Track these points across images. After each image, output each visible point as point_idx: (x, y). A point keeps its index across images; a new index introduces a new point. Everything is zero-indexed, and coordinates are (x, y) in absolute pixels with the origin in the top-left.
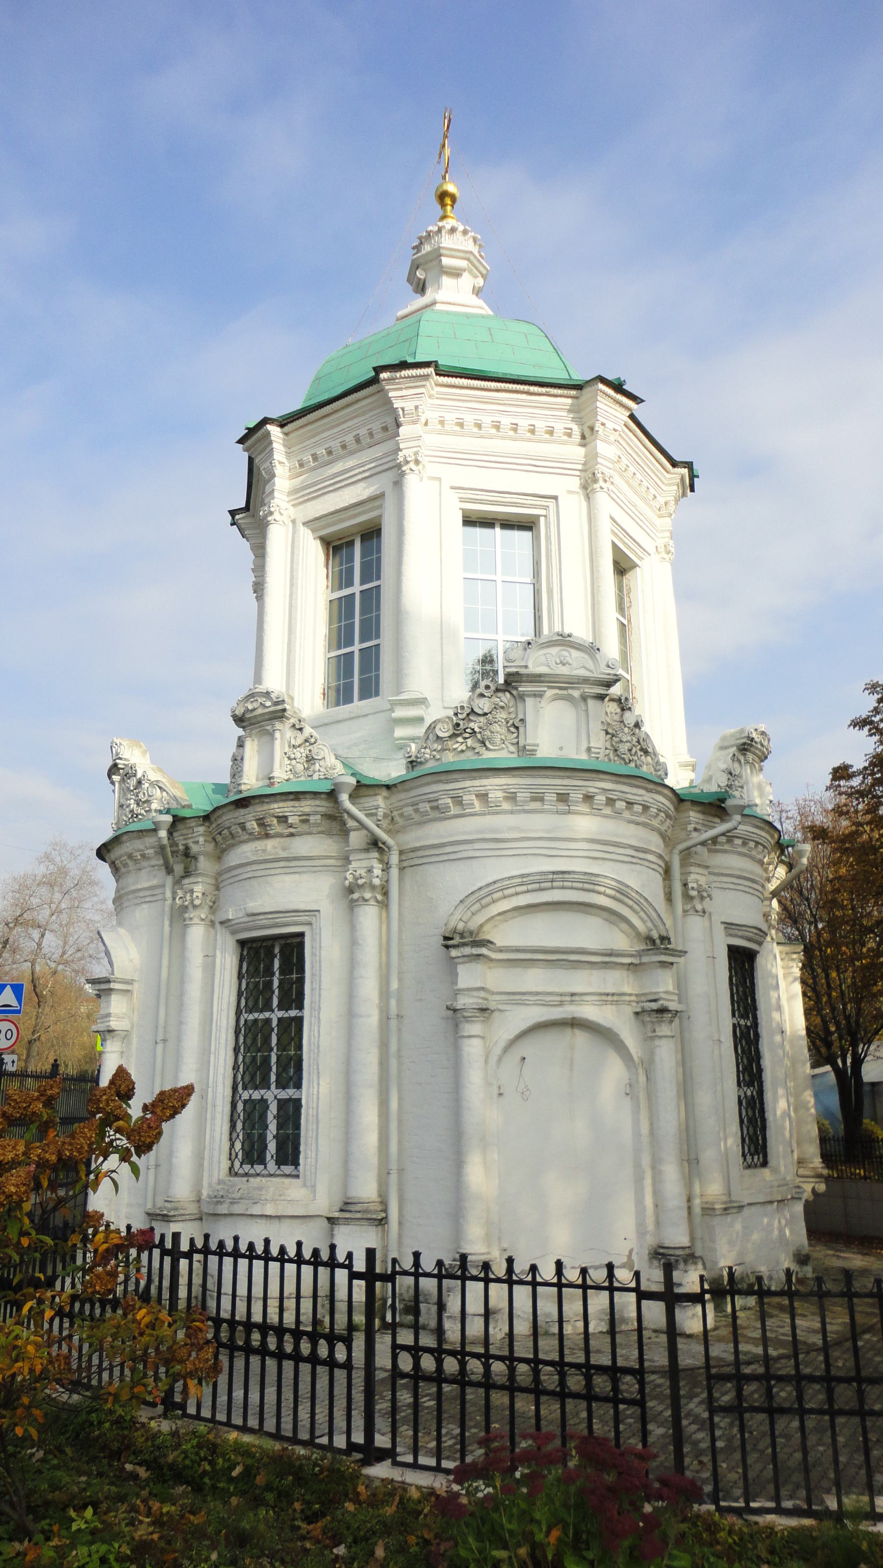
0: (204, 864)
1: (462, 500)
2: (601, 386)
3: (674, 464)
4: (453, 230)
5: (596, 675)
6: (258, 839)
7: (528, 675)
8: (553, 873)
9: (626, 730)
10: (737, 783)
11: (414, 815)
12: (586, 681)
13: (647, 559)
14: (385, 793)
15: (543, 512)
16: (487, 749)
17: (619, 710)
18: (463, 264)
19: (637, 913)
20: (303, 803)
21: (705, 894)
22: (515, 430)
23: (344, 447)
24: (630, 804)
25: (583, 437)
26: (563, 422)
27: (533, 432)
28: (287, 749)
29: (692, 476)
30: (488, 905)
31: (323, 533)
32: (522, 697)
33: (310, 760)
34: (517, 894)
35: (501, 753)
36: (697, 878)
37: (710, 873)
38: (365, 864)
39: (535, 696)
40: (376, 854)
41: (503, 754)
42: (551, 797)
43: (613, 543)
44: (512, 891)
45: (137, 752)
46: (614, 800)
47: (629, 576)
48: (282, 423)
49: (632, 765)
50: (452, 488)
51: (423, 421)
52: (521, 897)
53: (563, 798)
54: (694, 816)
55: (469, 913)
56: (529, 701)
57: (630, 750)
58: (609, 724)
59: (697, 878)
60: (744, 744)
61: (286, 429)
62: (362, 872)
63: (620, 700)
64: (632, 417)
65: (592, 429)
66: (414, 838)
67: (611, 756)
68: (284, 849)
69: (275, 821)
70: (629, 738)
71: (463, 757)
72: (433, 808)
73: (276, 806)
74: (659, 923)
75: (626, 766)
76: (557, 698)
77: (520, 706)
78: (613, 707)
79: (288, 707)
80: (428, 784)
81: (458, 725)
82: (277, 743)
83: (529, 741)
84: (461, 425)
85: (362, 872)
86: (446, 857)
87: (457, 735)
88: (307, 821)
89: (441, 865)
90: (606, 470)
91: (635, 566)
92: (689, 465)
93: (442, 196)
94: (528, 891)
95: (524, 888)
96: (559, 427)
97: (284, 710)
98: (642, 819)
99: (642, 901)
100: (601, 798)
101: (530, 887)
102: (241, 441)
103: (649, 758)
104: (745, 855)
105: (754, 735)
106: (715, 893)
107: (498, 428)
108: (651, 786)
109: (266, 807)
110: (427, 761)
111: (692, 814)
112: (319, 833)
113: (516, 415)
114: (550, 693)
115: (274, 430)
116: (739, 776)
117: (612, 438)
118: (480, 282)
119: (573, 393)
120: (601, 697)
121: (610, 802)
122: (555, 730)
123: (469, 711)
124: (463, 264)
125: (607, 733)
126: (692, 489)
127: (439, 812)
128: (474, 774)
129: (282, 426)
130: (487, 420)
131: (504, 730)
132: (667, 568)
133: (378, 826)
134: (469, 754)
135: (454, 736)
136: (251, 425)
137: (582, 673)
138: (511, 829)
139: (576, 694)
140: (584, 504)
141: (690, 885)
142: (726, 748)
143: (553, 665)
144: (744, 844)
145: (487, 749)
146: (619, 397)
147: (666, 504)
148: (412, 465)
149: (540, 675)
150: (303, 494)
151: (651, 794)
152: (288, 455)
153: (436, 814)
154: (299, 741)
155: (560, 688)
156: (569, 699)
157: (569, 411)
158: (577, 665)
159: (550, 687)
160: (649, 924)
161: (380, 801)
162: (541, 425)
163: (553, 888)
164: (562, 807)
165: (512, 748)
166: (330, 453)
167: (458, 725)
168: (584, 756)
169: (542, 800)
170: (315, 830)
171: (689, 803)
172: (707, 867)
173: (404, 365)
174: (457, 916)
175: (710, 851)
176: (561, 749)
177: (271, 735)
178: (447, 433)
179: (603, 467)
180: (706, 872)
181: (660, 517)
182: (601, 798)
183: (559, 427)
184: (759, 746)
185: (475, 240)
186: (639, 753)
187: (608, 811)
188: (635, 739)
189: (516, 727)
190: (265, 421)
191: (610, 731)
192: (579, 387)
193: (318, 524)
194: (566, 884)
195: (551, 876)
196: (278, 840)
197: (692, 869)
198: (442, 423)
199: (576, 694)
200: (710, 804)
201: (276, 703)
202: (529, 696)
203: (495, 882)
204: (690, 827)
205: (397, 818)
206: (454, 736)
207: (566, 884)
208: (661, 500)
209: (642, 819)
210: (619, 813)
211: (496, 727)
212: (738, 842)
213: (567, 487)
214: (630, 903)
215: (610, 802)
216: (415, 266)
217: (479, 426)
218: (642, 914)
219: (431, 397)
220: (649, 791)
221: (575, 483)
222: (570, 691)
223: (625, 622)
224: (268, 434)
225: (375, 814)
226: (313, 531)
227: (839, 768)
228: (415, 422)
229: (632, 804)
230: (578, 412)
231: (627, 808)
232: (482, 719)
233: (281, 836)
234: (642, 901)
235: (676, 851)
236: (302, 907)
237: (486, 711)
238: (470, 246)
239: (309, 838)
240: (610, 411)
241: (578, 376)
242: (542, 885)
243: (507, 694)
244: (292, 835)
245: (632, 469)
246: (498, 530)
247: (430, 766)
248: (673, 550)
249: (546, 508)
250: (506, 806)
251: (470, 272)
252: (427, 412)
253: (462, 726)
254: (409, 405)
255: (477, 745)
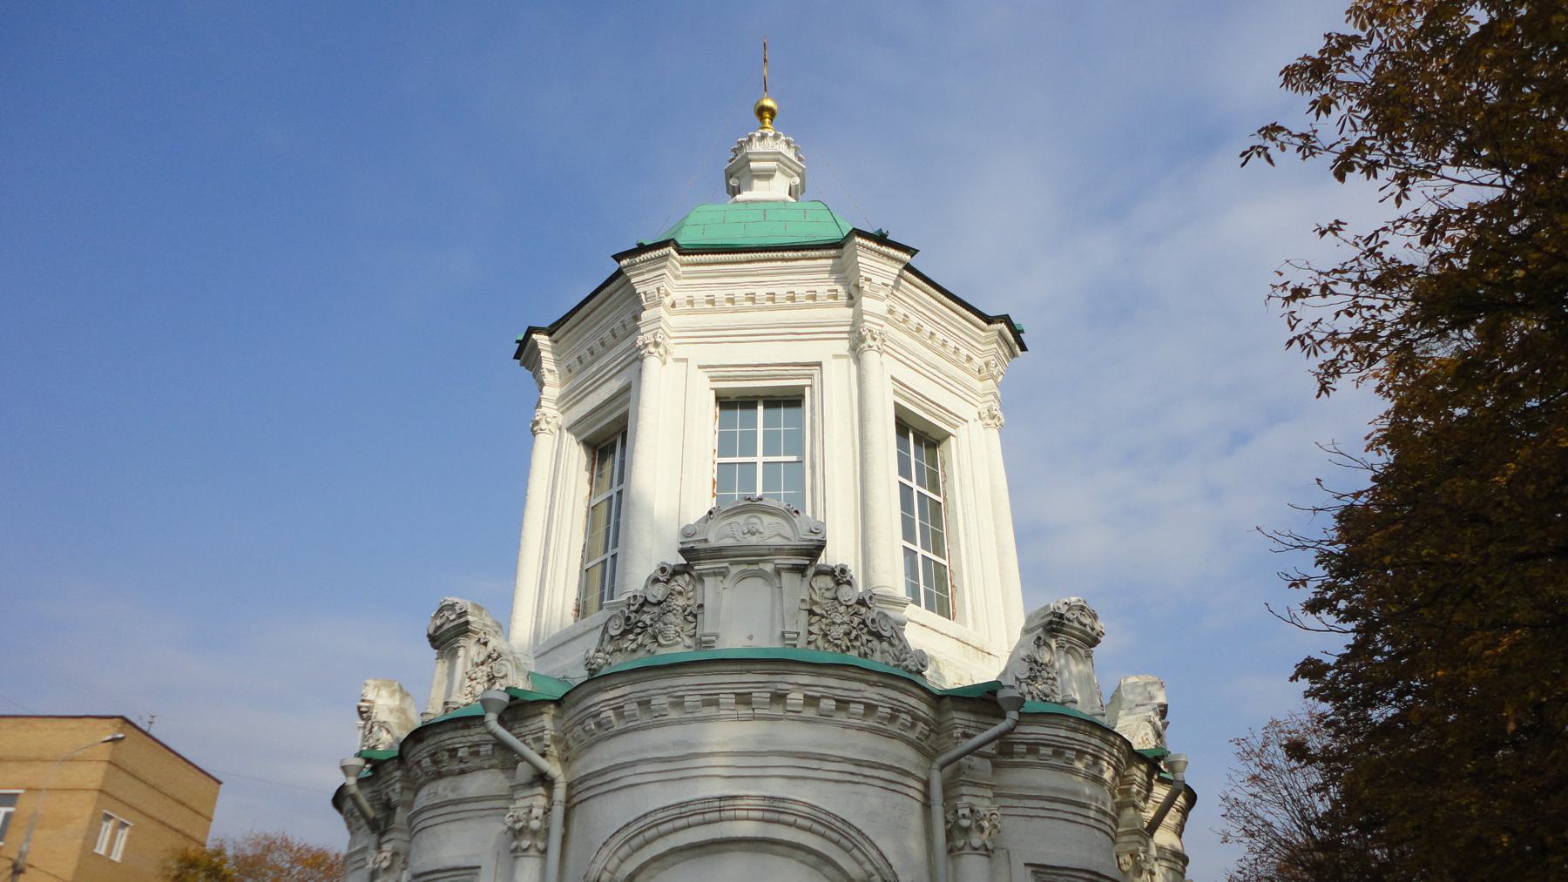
0: (401, 816)
1: (713, 379)
2: (858, 240)
3: (990, 320)
4: (763, 137)
5: (795, 543)
6: (433, 779)
7: (705, 550)
8: (720, 799)
9: (842, 609)
10: (1044, 674)
11: (583, 736)
12: (778, 550)
13: (963, 428)
14: (552, 709)
15: (807, 382)
16: (660, 645)
17: (831, 584)
18: (773, 165)
19: (848, 851)
20: (472, 731)
21: (986, 824)
22: (773, 300)
23: (603, 344)
24: (842, 704)
25: (850, 297)
26: (825, 285)
27: (793, 299)
28: (469, 667)
29: (1017, 333)
30: (640, 847)
31: (585, 436)
32: (700, 578)
33: (492, 679)
34: (676, 830)
35: (679, 647)
36: (975, 800)
37: (996, 795)
38: (526, 802)
39: (715, 574)
40: (541, 790)
41: (679, 649)
42: (727, 699)
43: (896, 404)
44: (669, 826)
45: (384, 692)
46: (817, 699)
47: (943, 447)
48: (550, 332)
49: (854, 653)
50: (700, 367)
51: (667, 301)
52: (680, 834)
53: (744, 699)
54: (960, 719)
55: (615, 861)
56: (709, 581)
57: (847, 634)
58: (816, 603)
59: (975, 800)
60: (1051, 622)
61: (555, 336)
62: (521, 813)
63: (833, 571)
64: (908, 268)
65: (857, 286)
66: (584, 766)
67: (820, 643)
68: (454, 790)
69: (446, 755)
70: (846, 619)
71: (635, 656)
72: (599, 725)
73: (446, 736)
74: (881, 864)
75: (851, 656)
76: (744, 576)
77: (699, 587)
78: (827, 582)
79: (470, 618)
80: (589, 694)
81: (628, 618)
82: (460, 661)
83: (707, 631)
84: (712, 302)
85: (521, 813)
86: (606, 788)
87: (630, 631)
88: (476, 754)
89: (602, 798)
90: (876, 328)
91: (950, 435)
92: (1006, 319)
93: (761, 111)
94: (689, 826)
95: (683, 822)
96: (822, 290)
97: (467, 623)
98: (870, 722)
99: (852, 833)
100: (796, 697)
101: (693, 820)
102: (517, 356)
103: (885, 644)
104: (1062, 769)
105: (1063, 610)
106: (1008, 824)
107: (753, 300)
108: (874, 678)
109: (437, 739)
110: (601, 667)
111: (954, 714)
112: (491, 767)
113: (774, 283)
114: (734, 570)
115: (542, 340)
116: (1050, 665)
117: (882, 294)
118: (797, 180)
119: (833, 252)
120: (800, 570)
121: (811, 701)
122: (743, 617)
123: (641, 600)
124: (773, 165)
125: (811, 613)
126: (1023, 348)
127: (605, 732)
128: (634, 676)
129: (550, 334)
130: (739, 293)
131: (679, 620)
132: (994, 435)
133: (543, 755)
134: (641, 653)
135: (624, 634)
136: (521, 337)
137: (778, 541)
138: (676, 744)
139: (769, 568)
140: (854, 367)
141: (960, 812)
142: (1032, 630)
143: (739, 536)
144: (1058, 752)
145: (660, 645)
146: (884, 249)
147: (987, 364)
148: (652, 349)
149: (720, 549)
150: (568, 400)
151: (876, 689)
152: (558, 362)
153: (602, 733)
154: (482, 658)
155: (749, 563)
156: (761, 574)
157: (831, 272)
158: (771, 532)
159: (732, 564)
160: (869, 867)
161: (547, 722)
162: (800, 291)
163: (721, 820)
164: (744, 711)
165: (689, 642)
166: (592, 353)
167: (628, 618)
168: (778, 645)
169: (716, 703)
170: (487, 763)
171: (948, 700)
172: (992, 787)
173: (642, 249)
174: (599, 865)
175: (995, 765)
176: (750, 638)
177: (453, 654)
178: (697, 312)
179: (870, 324)
180: (989, 793)
181: (981, 380)
182: (796, 697)
183: (822, 290)
184: (1076, 625)
185: (788, 143)
186: (865, 637)
187: (810, 713)
188: (856, 620)
189: (693, 615)
190: (531, 330)
191: (816, 609)
192: (837, 245)
193: (580, 427)
194: (739, 813)
195: (717, 804)
196: (450, 779)
197: (964, 790)
198: (691, 302)
199: (769, 568)
200: (982, 699)
201: (460, 615)
202: (708, 575)
203: (645, 816)
204: (957, 733)
205: (571, 742)
206: (624, 634)
207: (739, 813)
208: (978, 361)
209: (870, 722)
210: (826, 715)
211: (670, 617)
212: (1043, 750)
213: (831, 352)
214: (836, 836)
215: (811, 701)
216: (729, 175)
217: (732, 301)
218: (855, 852)
219: (677, 277)
220: (874, 684)
221: (843, 346)
222: (762, 566)
223: (940, 500)
224: (535, 343)
225: (540, 739)
226: (577, 435)
227: (1303, 664)
228: (658, 304)
229: (848, 702)
230: (842, 271)
231: (838, 708)
232: (656, 610)
233: (451, 774)
234: (852, 833)
235: (936, 766)
236: (462, 863)
237: (660, 598)
238: (782, 148)
239: (480, 774)
240: (875, 267)
241: (834, 234)
242: (707, 816)
243: (687, 577)
244: (462, 772)
245: (927, 328)
246: (760, 408)
247: (605, 671)
248: (999, 414)
249: (810, 376)
250: (674, 715)
251: (783, 172)
252: (675, 296)
253: (633, 620)
254: (651, 288)
255: (648, 641)
